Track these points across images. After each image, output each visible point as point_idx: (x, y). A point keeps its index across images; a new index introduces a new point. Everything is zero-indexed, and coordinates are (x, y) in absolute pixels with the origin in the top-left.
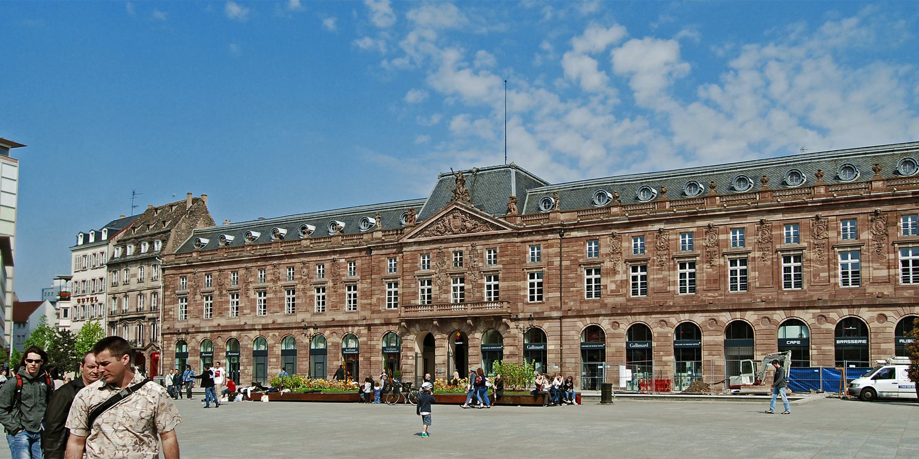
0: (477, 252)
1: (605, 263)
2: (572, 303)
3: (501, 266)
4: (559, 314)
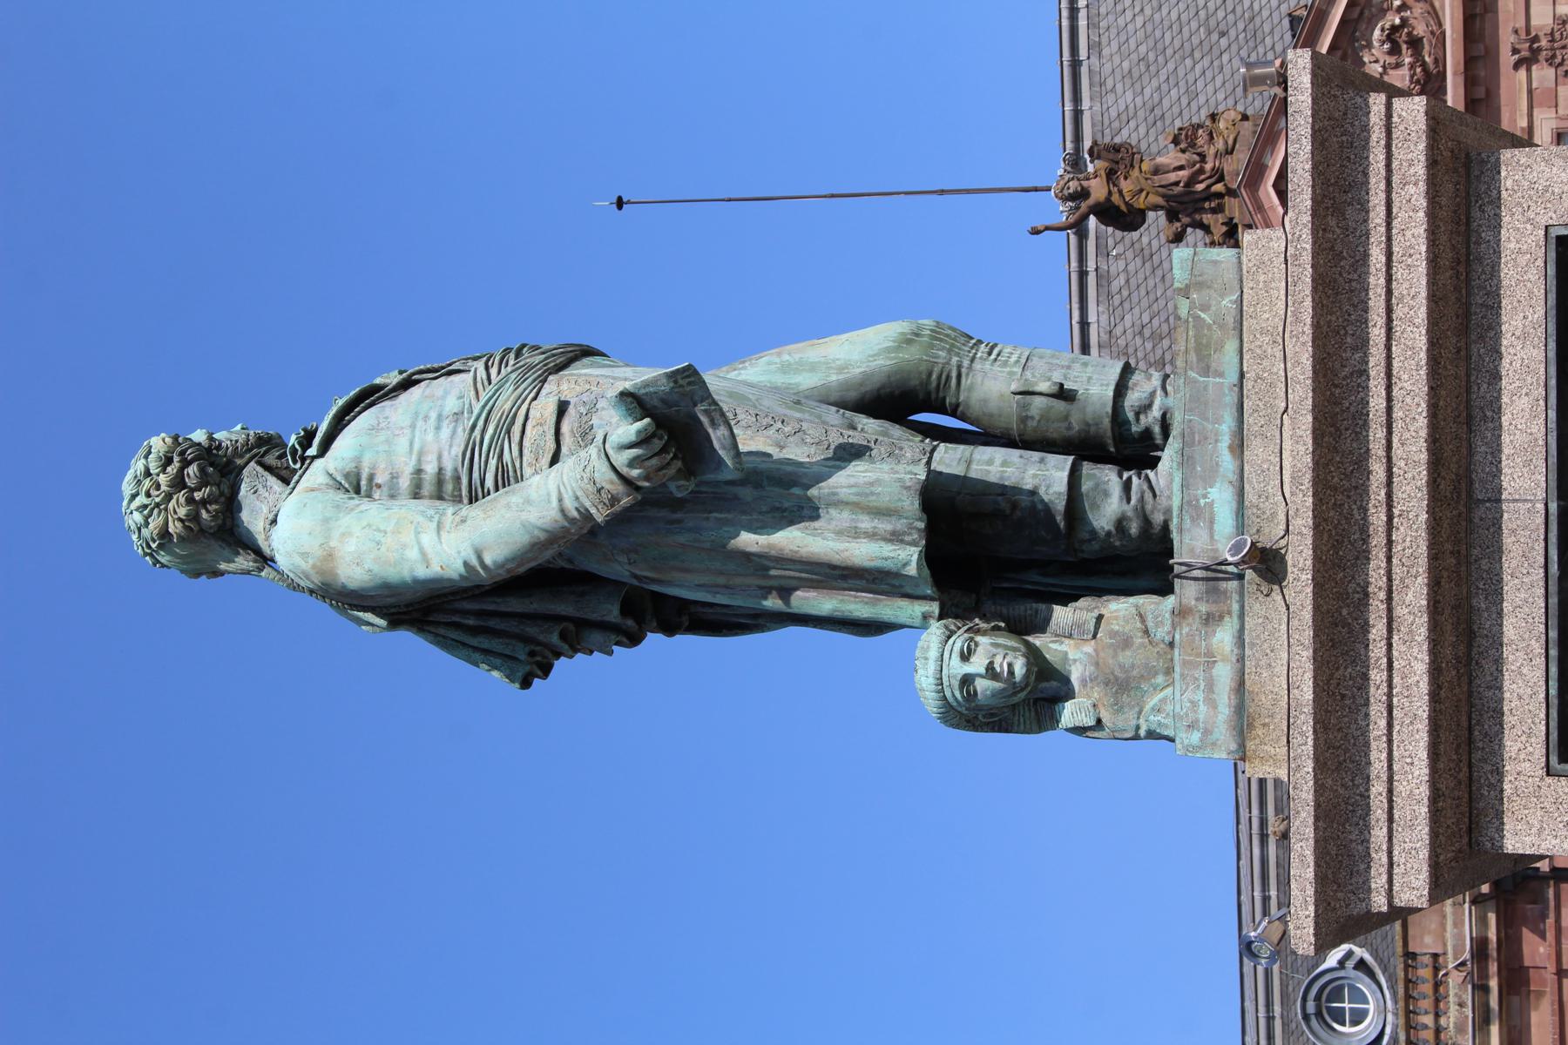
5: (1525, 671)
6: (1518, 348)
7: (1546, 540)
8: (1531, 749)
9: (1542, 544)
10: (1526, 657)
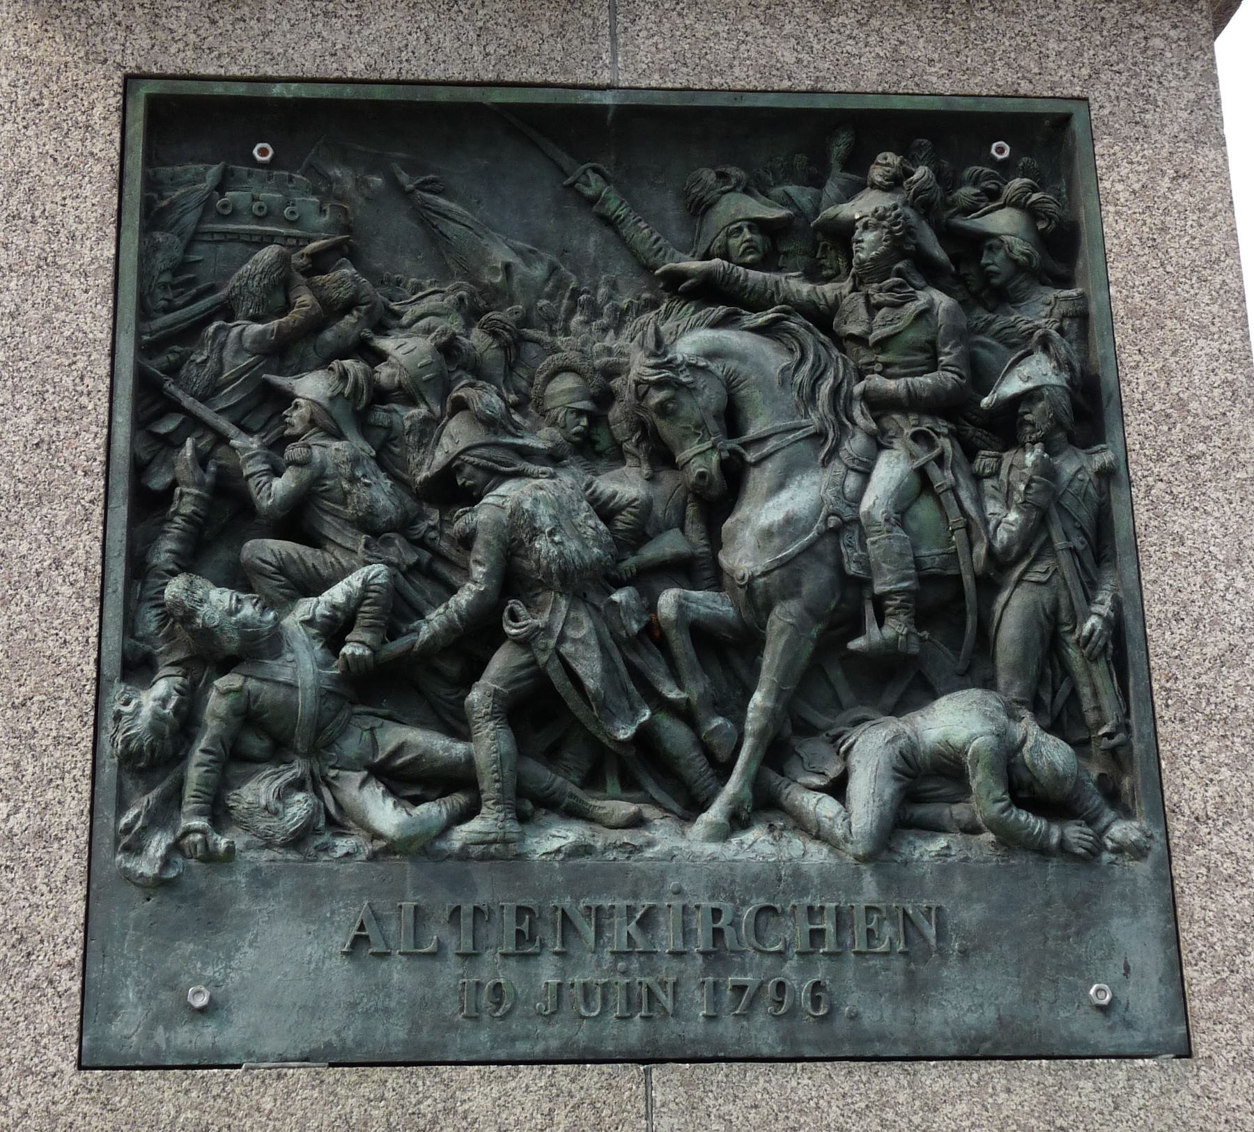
5: (314, 44)
6: (878, 50)
8: (173, 50)
9: (539, 79)
10: (339, 46)
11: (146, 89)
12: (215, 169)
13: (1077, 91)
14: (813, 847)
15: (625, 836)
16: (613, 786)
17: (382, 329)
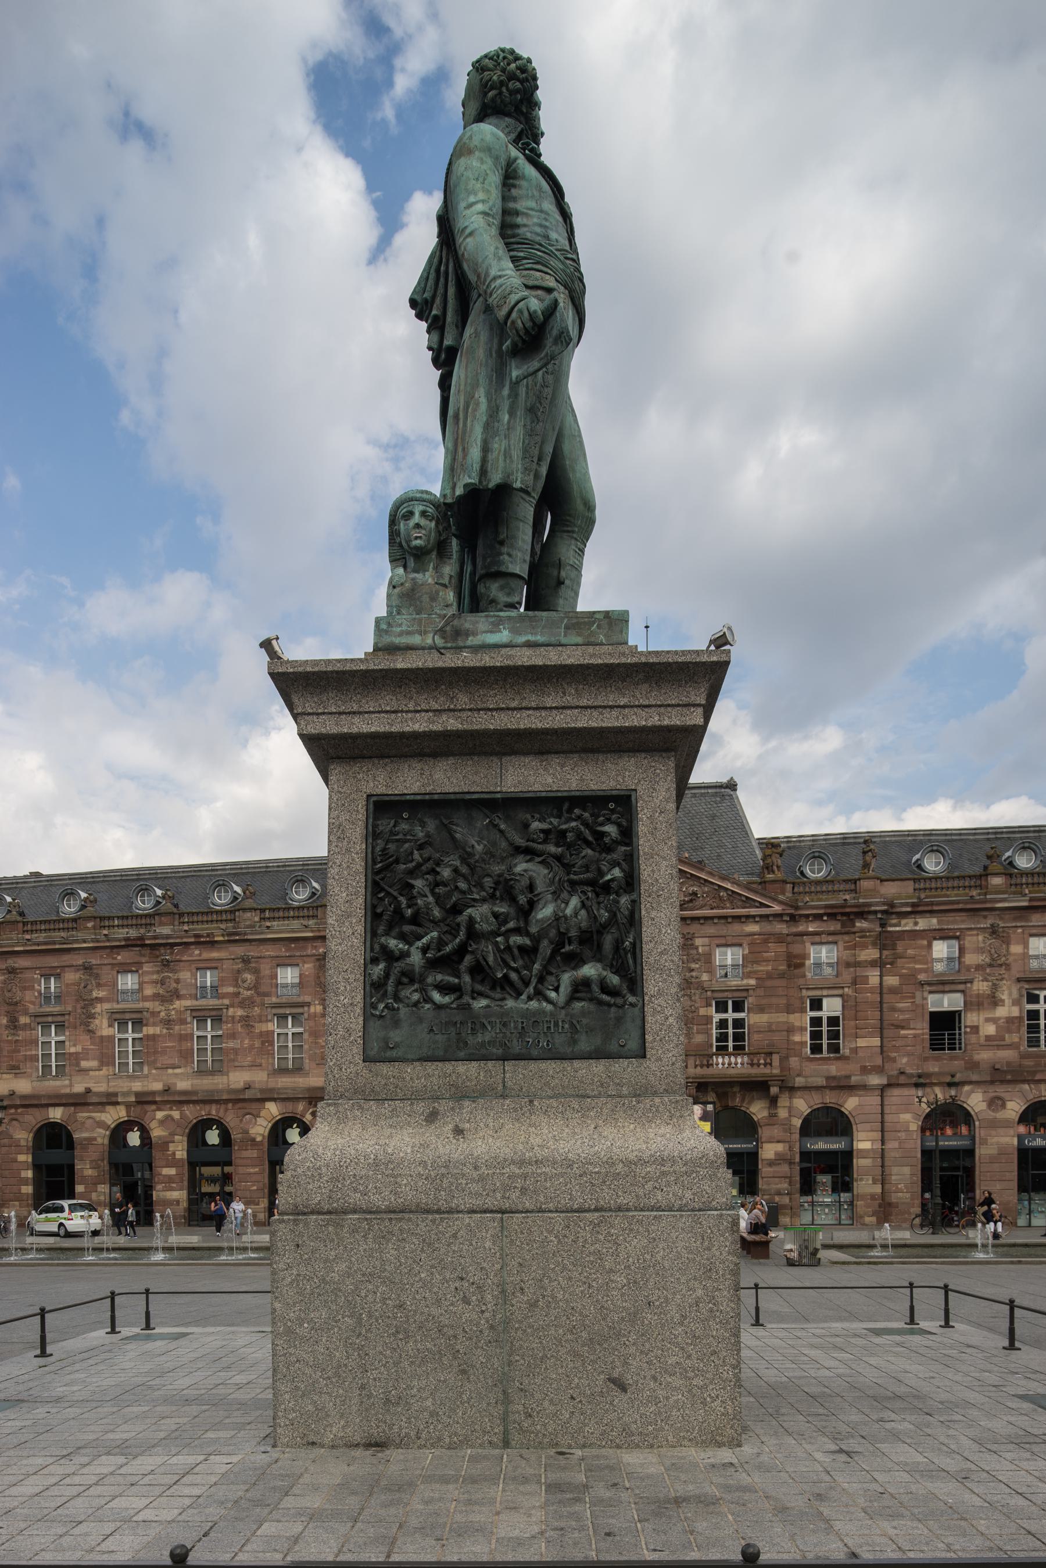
0: (695, 952)
1: (975, 983)
2: (905, 1060)
3: (752, 982)
4: (875, 1080)
7: (482, 792)
11: (375, 798)
12: (393, 822)
13: (633, 787)
14: (549, 1005)
15: (499, 1003)
16: (499, 990)
17: (438, 865)
